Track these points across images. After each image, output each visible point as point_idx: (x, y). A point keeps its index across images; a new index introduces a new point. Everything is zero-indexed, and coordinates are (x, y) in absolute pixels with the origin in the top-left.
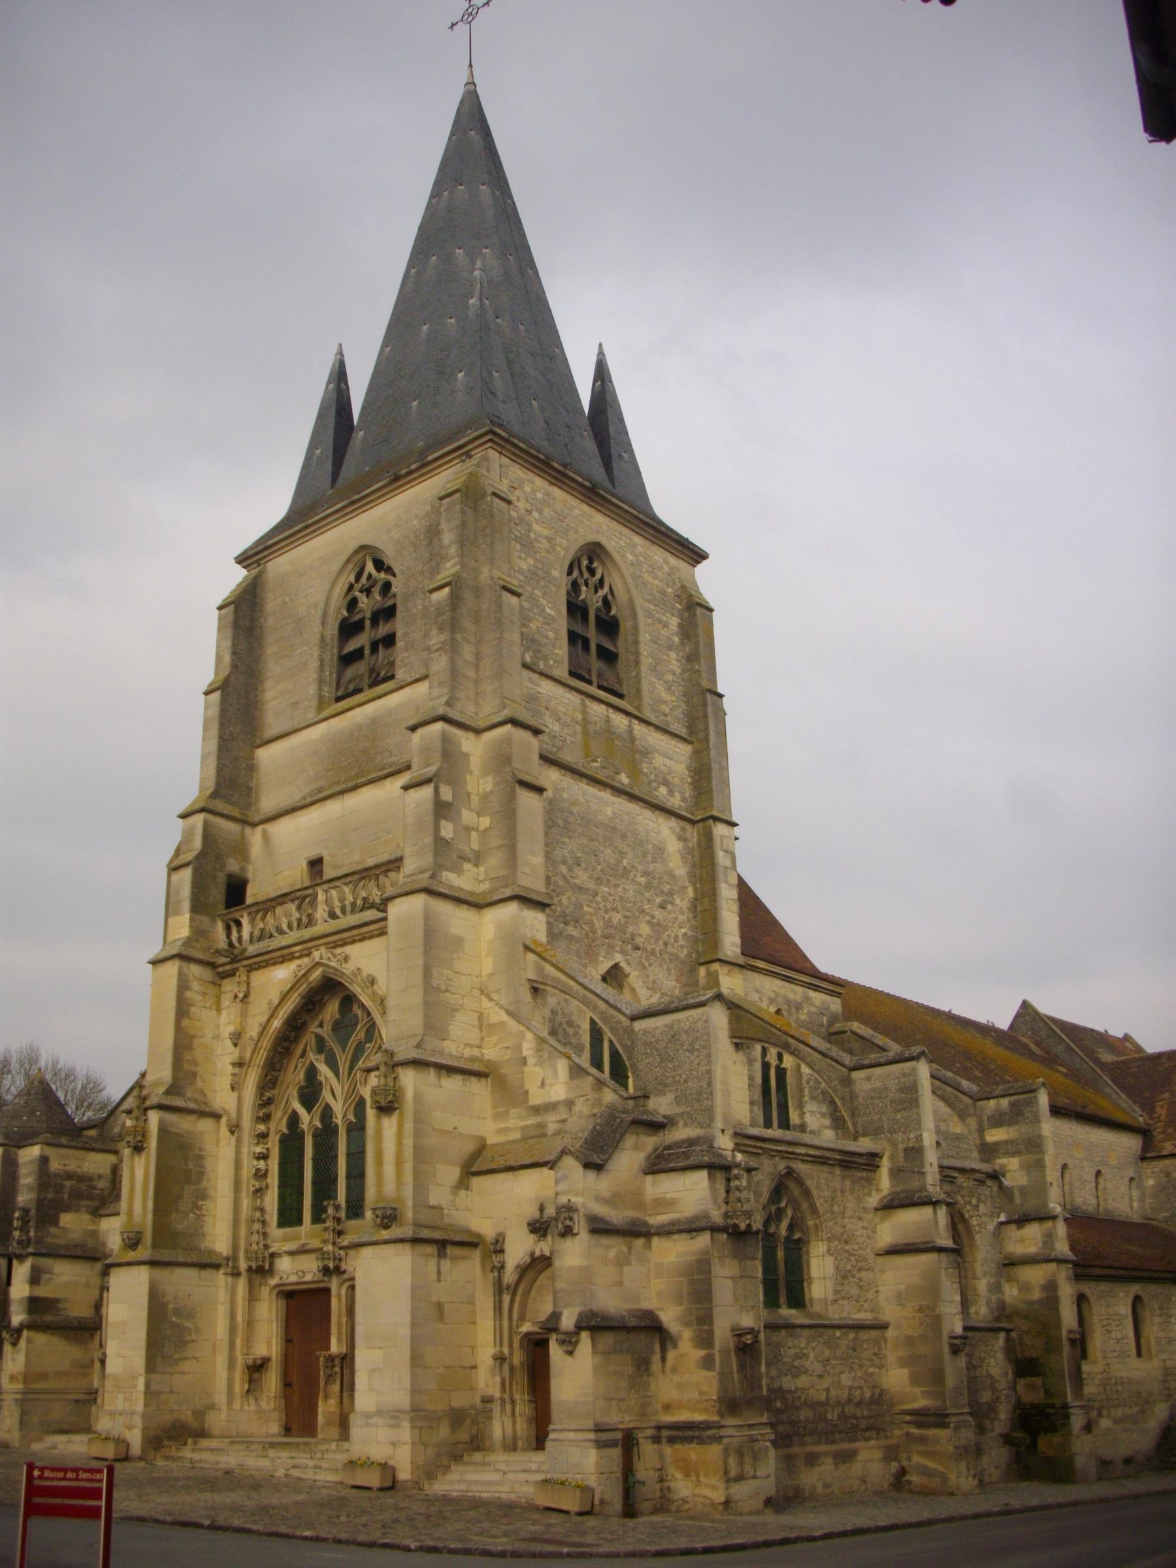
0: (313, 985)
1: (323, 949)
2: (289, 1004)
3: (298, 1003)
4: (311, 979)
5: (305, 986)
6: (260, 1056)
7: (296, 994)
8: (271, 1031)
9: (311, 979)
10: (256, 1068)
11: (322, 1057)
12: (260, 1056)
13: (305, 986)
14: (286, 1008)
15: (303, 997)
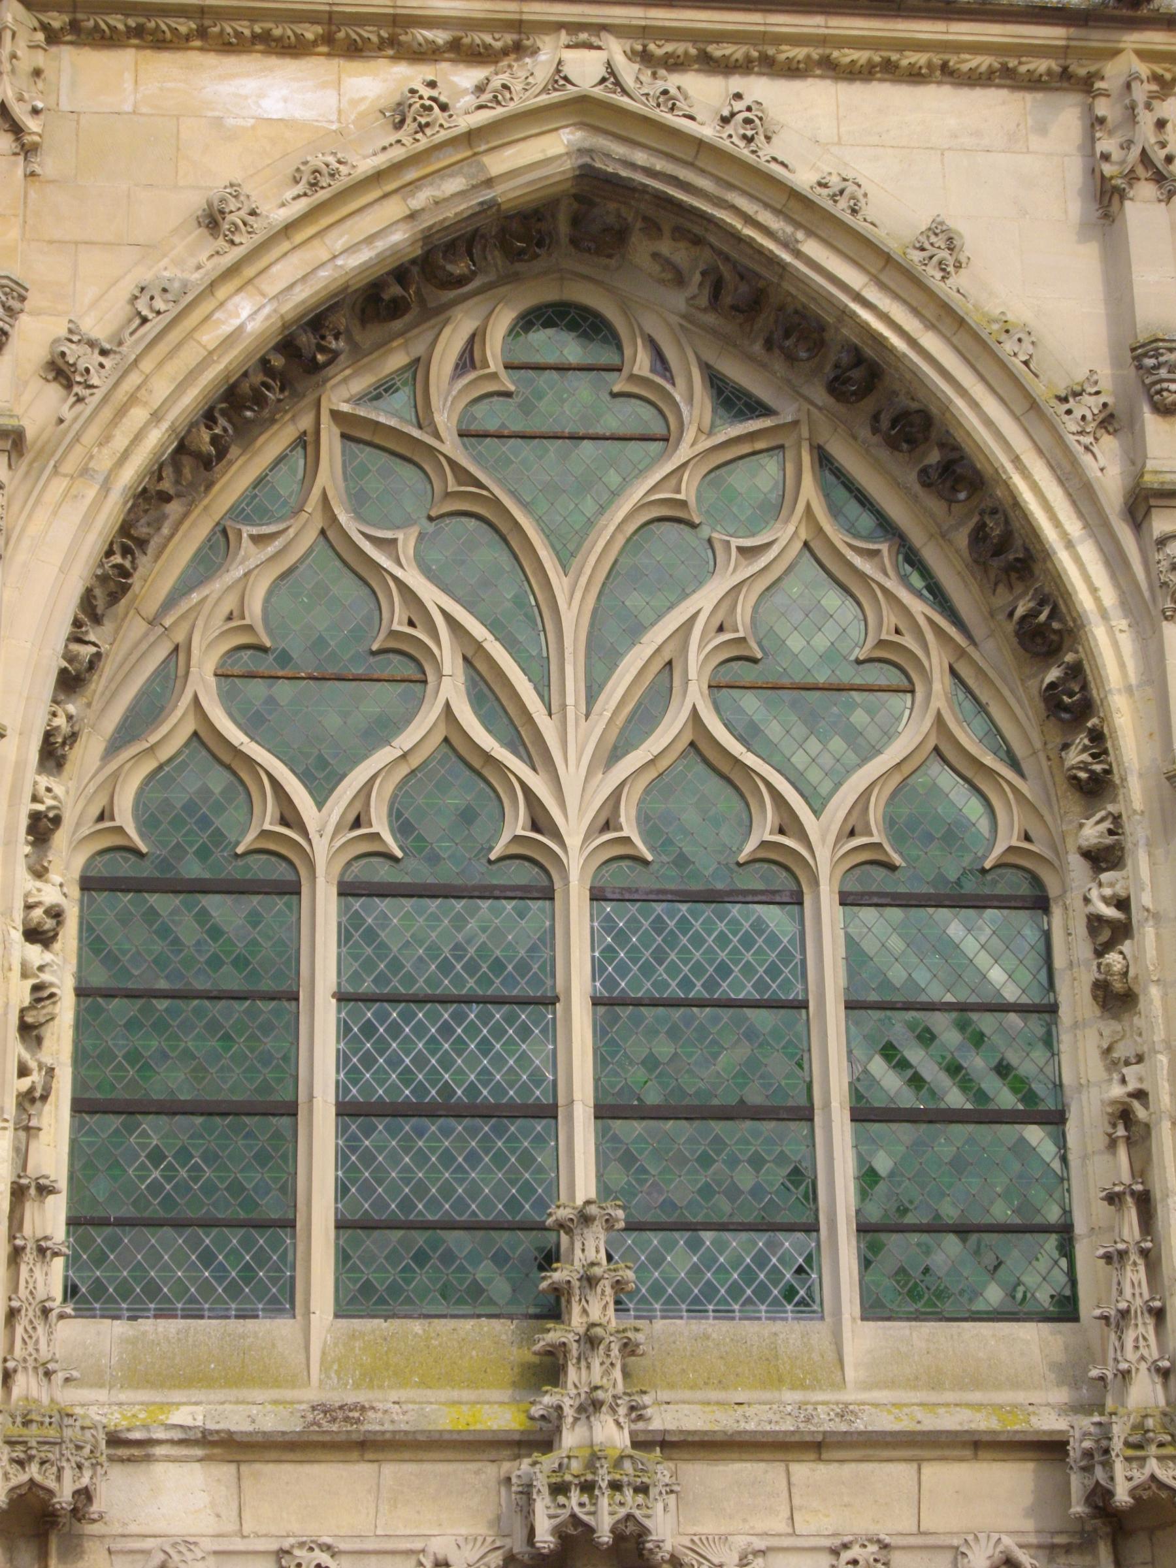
0: (503, 193)
1: (616, 49)
2: (338, 240)
3: (394, 250)
4: (500, 162)
5: (453, 185)
6: (120, 441)
7: (394, 209)
8: (210, 337)
9: (500, 162)
10: (91, 492)
11: (407, 541)
12: (120, 441)
13: (453, 185)
14: (319, 252)
15: (427, 237)
